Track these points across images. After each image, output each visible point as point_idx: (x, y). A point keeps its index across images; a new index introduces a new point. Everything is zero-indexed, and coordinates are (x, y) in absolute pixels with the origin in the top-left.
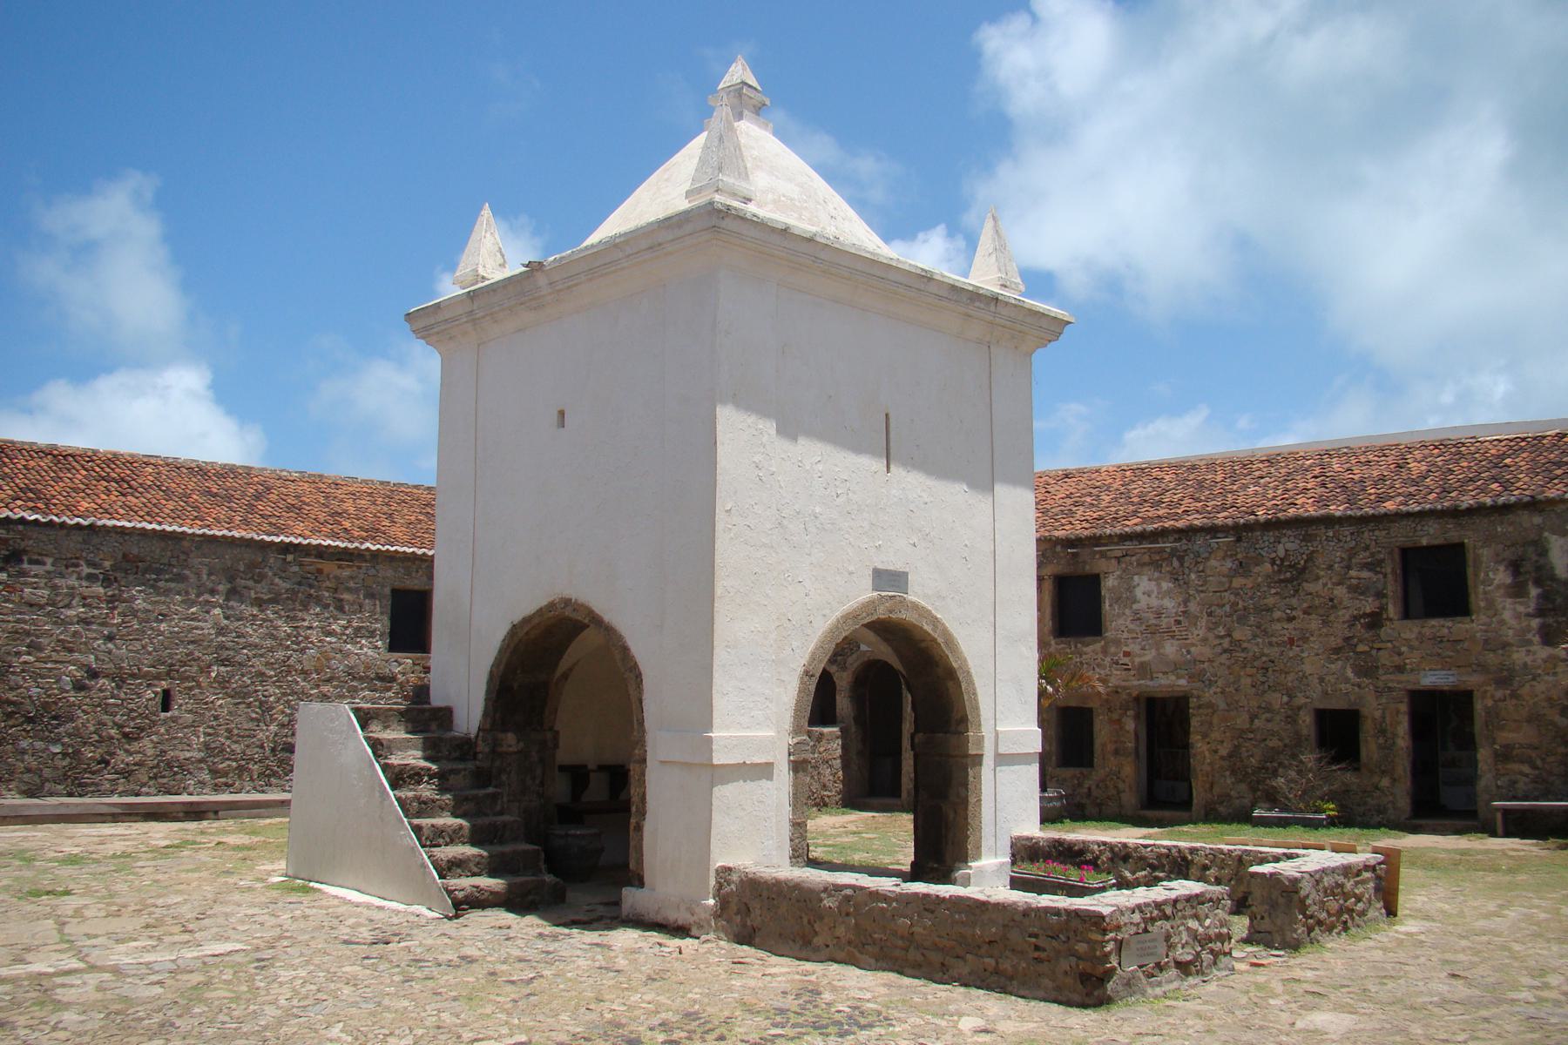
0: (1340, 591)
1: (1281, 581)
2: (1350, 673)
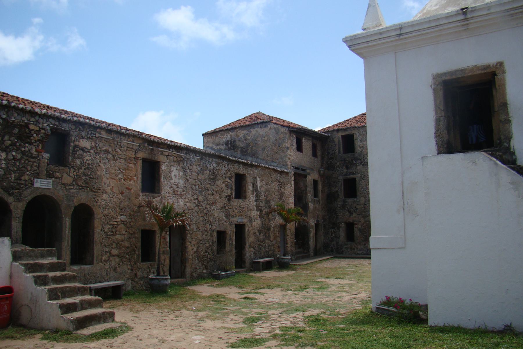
2: (224, 218)
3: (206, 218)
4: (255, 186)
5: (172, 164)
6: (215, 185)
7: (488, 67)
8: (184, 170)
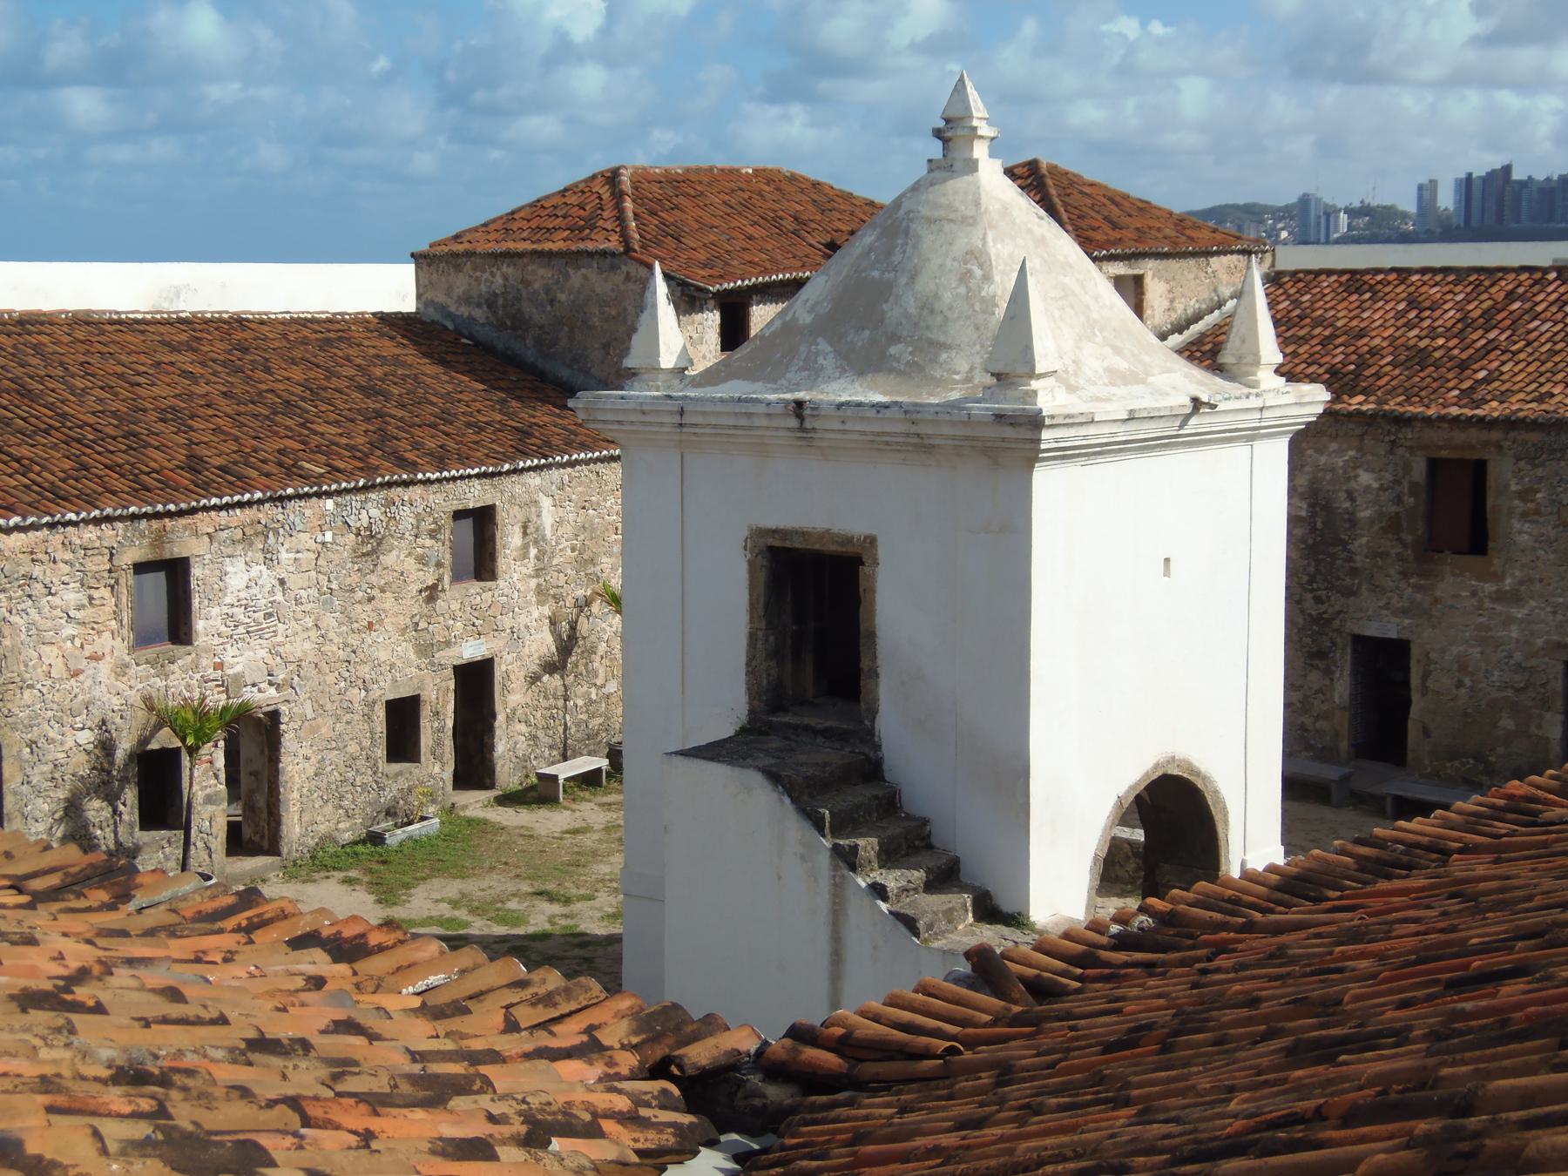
0: (410, 564)
1: (364, 555)
2: (413, 657)
3: (346, 674)
4: (531, 530)
5: (229, 551)
6: (379, 568)
7: (848, 540)
8: (269, 556)
